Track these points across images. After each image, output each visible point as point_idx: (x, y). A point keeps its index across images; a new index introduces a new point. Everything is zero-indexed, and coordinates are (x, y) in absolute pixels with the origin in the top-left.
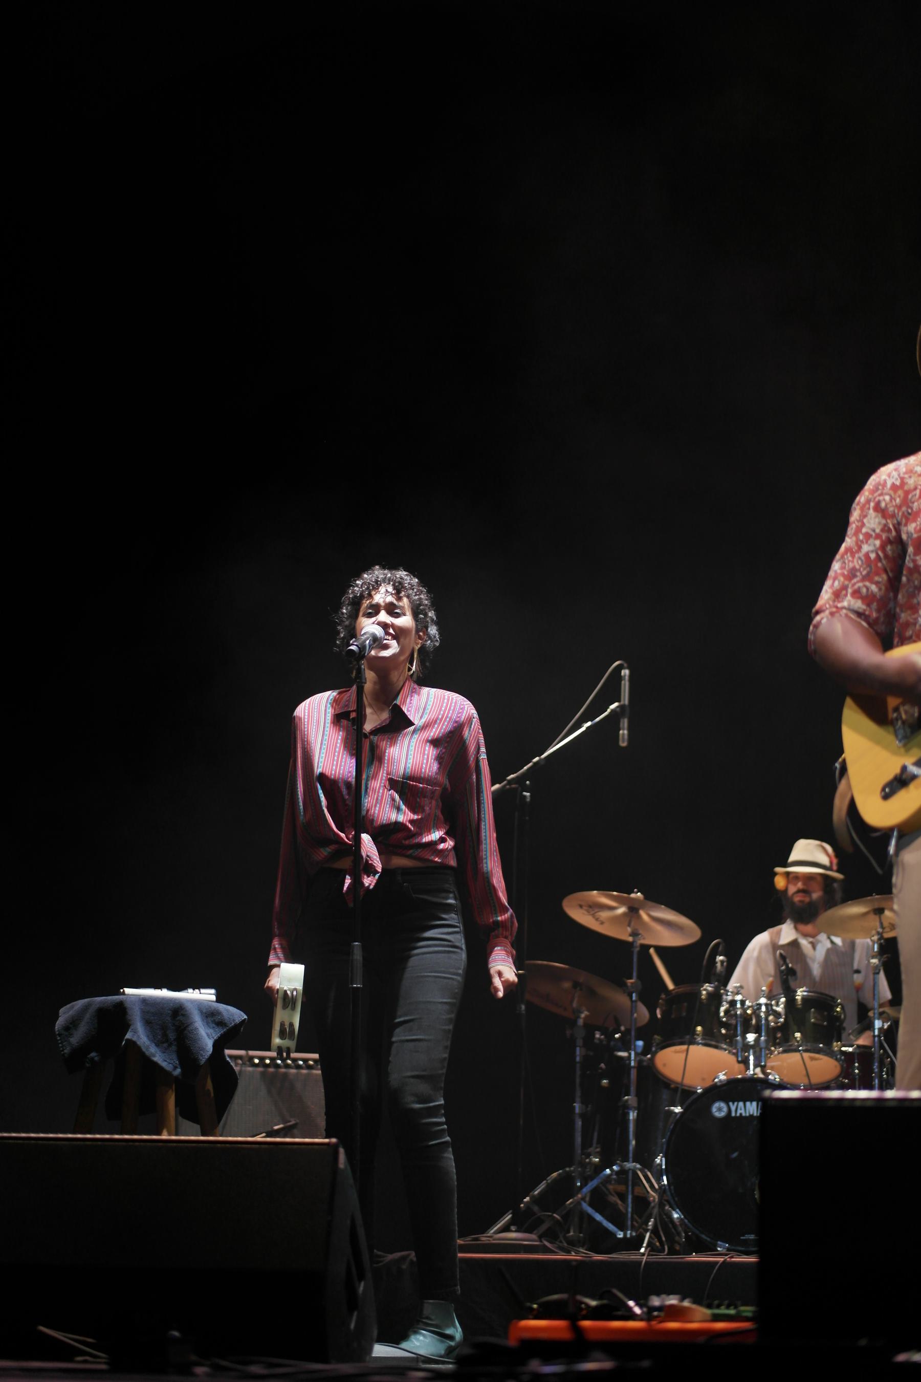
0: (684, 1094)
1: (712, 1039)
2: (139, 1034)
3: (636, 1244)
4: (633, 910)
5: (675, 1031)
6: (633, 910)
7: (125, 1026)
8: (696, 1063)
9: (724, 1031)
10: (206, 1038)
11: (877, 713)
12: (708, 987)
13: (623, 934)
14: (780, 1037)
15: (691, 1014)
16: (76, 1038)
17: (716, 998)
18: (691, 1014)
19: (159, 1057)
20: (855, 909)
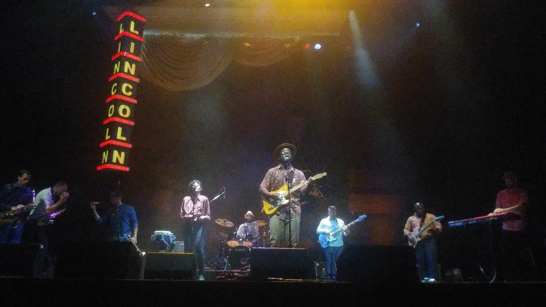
0: (230, 247)
1: (235, 240)
2: (163, 239)
3: (224, 269)
4: (225, 221)
5: (230, 239)
6: (225, 221)
7: (161, 238)
8: (233, 243)
9: (237, 239)
10: (172, 240)
11: (268, 201)
12: (235, 233)
13: (223, 225)
14: (244, 240)
15: (232, 236)
16: (154, 239)
17: (236, 234)
18: (232, 236)
19: (165, 242)
20: (255, 222)
